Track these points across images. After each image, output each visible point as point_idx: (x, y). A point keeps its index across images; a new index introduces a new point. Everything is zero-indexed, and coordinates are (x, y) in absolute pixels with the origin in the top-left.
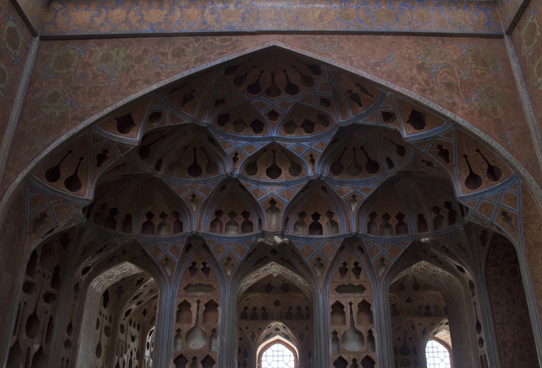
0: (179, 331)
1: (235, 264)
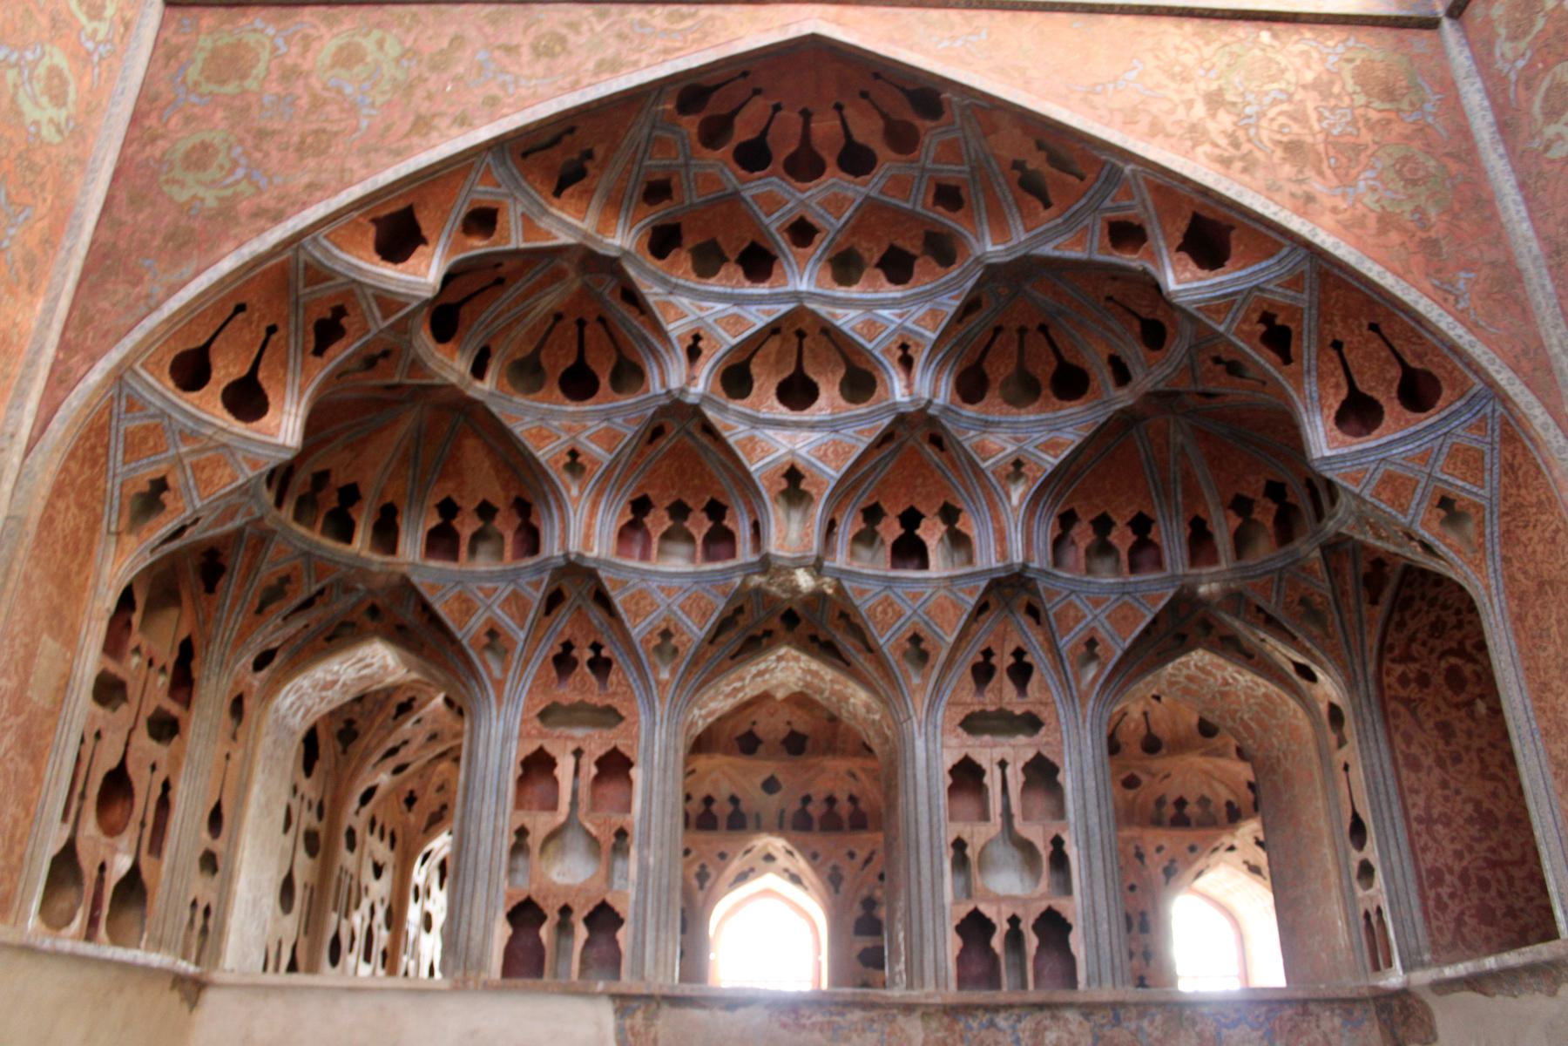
0: (522, 832)
1: (681, 649)
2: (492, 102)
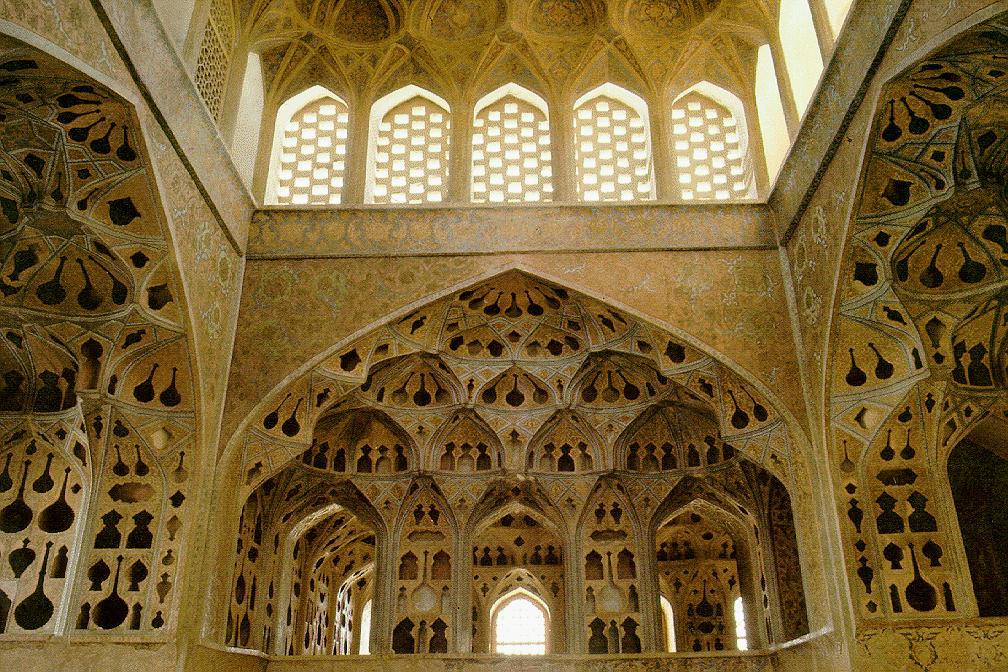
2: (386, 306)
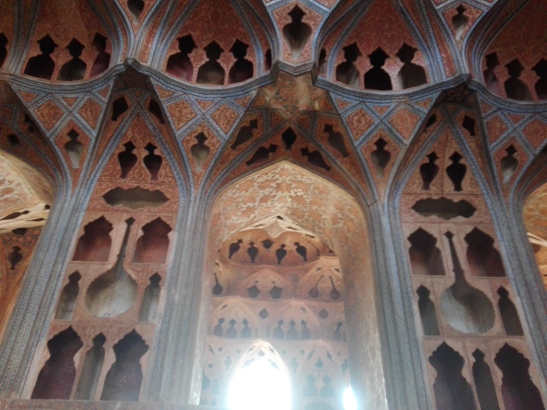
1: (212, 148)
